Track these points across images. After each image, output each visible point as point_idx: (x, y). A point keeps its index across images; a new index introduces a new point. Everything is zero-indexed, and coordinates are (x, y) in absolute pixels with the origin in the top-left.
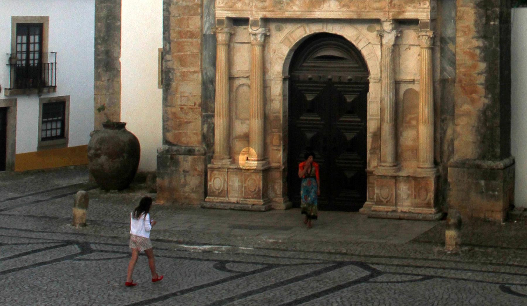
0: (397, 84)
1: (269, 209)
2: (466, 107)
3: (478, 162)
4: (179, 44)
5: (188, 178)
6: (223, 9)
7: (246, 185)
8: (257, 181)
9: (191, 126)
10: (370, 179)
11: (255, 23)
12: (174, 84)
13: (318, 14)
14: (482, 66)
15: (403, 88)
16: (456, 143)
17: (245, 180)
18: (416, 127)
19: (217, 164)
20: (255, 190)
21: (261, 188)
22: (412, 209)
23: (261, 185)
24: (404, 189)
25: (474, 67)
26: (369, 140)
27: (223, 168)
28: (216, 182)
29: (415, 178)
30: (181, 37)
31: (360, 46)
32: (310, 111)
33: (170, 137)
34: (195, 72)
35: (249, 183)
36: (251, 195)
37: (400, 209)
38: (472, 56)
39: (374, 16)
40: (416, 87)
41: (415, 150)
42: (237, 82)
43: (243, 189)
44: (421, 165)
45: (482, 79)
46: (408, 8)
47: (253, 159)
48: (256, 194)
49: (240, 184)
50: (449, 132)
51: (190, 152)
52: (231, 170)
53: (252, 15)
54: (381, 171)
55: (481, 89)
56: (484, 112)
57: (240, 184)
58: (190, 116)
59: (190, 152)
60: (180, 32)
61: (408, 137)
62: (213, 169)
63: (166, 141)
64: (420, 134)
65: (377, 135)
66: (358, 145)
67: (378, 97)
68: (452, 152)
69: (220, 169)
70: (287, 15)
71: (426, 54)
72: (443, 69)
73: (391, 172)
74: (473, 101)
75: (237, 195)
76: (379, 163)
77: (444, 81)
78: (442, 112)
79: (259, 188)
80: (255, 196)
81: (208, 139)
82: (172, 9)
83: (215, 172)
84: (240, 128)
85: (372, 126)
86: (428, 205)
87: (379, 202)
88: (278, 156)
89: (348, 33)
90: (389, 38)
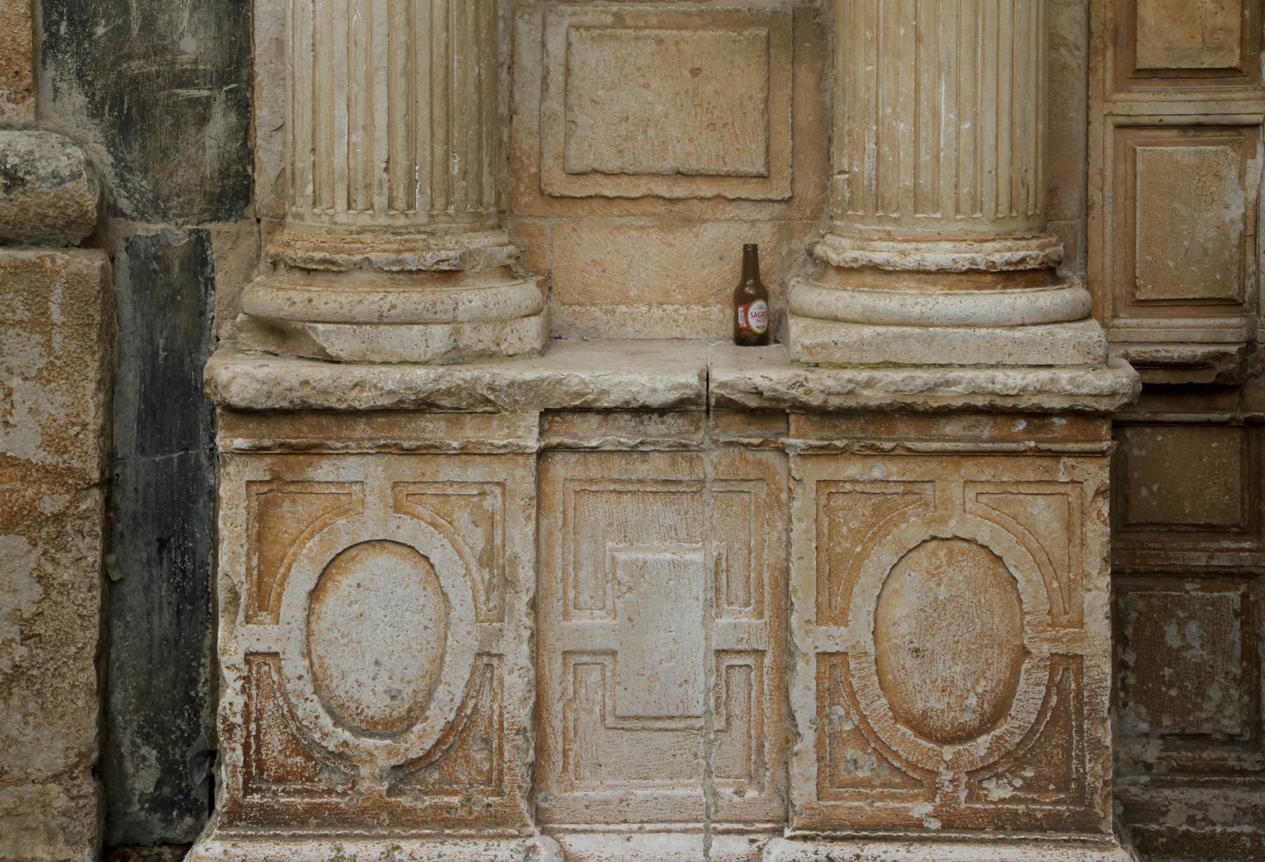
7: (832, 638)
17: (834, 572)
20: (999, 709)
21: (1101, 669)
23: (1099, 628)
27: (483, 405)
35: (903, 610)
36: (922, 780)
43: (803, 699)
47: (940, 255)
48: (1009, 760)
49: (741, 623)
52: (590, 432)
57: (741, 623)
62: (299, 429)
69: (433, 429)
75: (691, 791)
79: (1067, 663)
80: (998, 791)
83: (355, 473)
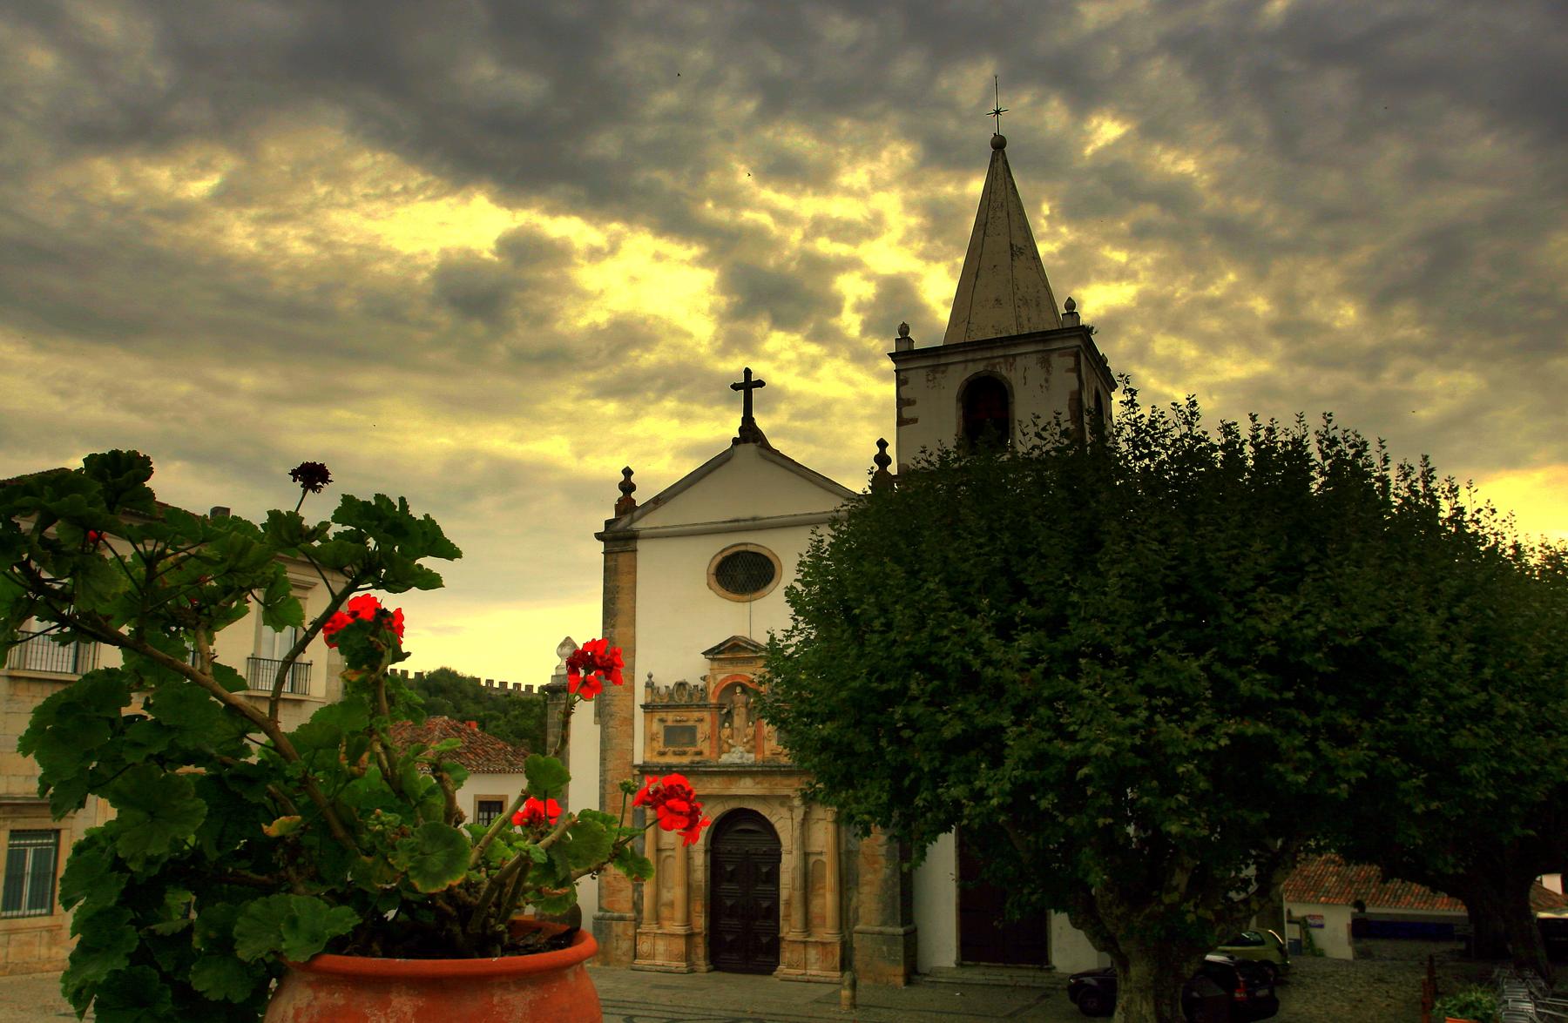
0: (806, 855)
1: (692, 971)
2: (869, 877)
8: (680, 946)
10: (784, 945)
13: (734, 791)
15: (812, 859)
16: (861, 911)
18: (824, 896)
19: (644, 928)
24: (813, 954)
26: (782, 908)
28: (644, 946)
29: (823, 944)
31: (773, 820)
32: (730, 881)
33: (604, 902)
39: (786, 792)
40: (824, 858)
41: (824, 918)
42: (664, 854)
44: (827, 932)
45: (883, 850)
50: (854, 902)
51: (621, 919)
54: (791, 936)
55: (882, 860)
56: (885, 881)
59: (621, 919)
61: (816, 906)
63: (600, 909)
64: (826, 901)
65: (788, 903)
66: (772, 913)
67: (789, 864)
68: (857, 920)
71: (831, 827)
72: (848, 841)
73: (801, 938)
74: (875, 871)
76: (790, 929)
77: (849, 852)
78: (847, 882)
81: (637, 906)
82: (608, 787)
84: (666, 896)
85: (784, 894)
86: (834, 969)
87: (790, 966)
88: (700, 923)
89: (763, 810)
90: (799, 813)
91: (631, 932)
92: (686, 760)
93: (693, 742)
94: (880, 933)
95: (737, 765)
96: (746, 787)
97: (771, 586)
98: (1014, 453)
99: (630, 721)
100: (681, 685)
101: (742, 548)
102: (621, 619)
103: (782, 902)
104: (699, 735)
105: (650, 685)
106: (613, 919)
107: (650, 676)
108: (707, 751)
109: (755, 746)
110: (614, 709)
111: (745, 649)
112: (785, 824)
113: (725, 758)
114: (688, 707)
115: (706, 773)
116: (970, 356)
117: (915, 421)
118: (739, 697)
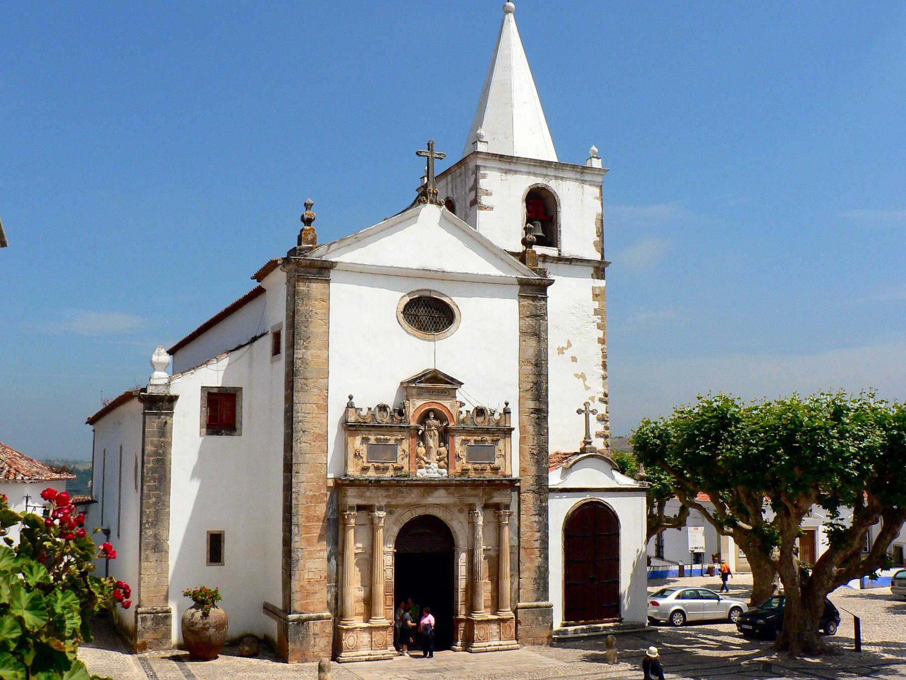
2: (527, 565)
3: (535, 604)
4: (307, 527)
5: (317, 640)
6: (354, 497)
9: (318, 596)
11: (380, 509)
12: (301, 561)
14: (538, 535)
22: (501, 643)
25: (532, 536)
28: (348, 640)
30: (309, 521)
34: (321, 550)
37: (493, 643)
38: (532, 528)
45: (537, 544)
46: (495, 494)
53: (378, 502)
58: (317, 587)
59: (319, 618)
60: (307, 517)
62: (348, 630)
70: (408, 500)
74: (532, 560)
83: (351, 634)
91: (329, 629)
92: (388, 475)
93: (394, 457)
94: (538, 607)
95: (431, 479)
96: (440, 497)
97: (452, 328)
98: (560, 251)
99: (324, 437)
100: (383, 408)
101: (427, 294)
102: (315, 342)
103: (460, 590)
104: (400, 453)
105: (350, 406)
106: (309, 619)
107: (351, 398)
108: (406, 468)
109: (446, 462)
110: (307, 426)
111: (440, 381)
112: (458, 526)
113: (422, 474)
114: (389, 429)
115: (408, 485)
116: (532, 169)
117: (492, 209)
118: (433, 422)
